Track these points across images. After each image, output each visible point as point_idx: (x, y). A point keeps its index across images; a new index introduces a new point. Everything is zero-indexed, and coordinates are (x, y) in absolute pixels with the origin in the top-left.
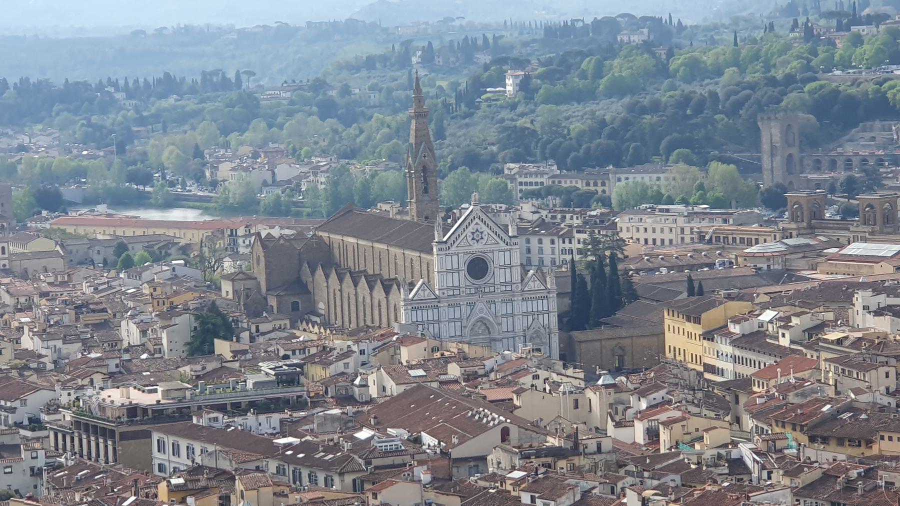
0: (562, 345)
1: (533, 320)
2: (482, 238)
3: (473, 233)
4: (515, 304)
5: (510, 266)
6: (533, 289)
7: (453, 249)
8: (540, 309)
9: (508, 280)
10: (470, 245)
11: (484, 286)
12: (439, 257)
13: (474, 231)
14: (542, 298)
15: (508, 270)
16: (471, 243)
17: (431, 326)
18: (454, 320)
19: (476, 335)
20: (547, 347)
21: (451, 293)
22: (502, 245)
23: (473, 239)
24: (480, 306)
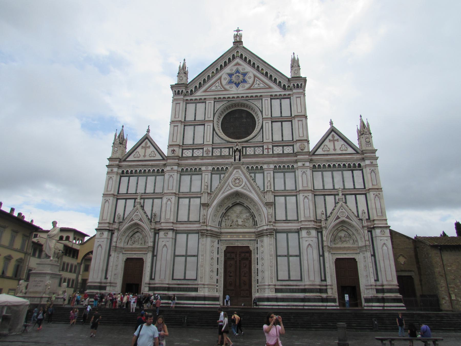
0: (402, 260)
1: (336, 203)
2: (244, 81)
3: (230, 75)
4: (299, 173)
6: (334, 152)
7: (199, 94)
8: (349, 185)
10: (226, 90)
12: (175, 102)
14: (352, 168)
15: (287, 125)
16: (227, 87)
17: (148, 203)
18: (190, 196)
20: (370, 259)
21: (188, 153)
22: (276, 89)
23: (230, 82)
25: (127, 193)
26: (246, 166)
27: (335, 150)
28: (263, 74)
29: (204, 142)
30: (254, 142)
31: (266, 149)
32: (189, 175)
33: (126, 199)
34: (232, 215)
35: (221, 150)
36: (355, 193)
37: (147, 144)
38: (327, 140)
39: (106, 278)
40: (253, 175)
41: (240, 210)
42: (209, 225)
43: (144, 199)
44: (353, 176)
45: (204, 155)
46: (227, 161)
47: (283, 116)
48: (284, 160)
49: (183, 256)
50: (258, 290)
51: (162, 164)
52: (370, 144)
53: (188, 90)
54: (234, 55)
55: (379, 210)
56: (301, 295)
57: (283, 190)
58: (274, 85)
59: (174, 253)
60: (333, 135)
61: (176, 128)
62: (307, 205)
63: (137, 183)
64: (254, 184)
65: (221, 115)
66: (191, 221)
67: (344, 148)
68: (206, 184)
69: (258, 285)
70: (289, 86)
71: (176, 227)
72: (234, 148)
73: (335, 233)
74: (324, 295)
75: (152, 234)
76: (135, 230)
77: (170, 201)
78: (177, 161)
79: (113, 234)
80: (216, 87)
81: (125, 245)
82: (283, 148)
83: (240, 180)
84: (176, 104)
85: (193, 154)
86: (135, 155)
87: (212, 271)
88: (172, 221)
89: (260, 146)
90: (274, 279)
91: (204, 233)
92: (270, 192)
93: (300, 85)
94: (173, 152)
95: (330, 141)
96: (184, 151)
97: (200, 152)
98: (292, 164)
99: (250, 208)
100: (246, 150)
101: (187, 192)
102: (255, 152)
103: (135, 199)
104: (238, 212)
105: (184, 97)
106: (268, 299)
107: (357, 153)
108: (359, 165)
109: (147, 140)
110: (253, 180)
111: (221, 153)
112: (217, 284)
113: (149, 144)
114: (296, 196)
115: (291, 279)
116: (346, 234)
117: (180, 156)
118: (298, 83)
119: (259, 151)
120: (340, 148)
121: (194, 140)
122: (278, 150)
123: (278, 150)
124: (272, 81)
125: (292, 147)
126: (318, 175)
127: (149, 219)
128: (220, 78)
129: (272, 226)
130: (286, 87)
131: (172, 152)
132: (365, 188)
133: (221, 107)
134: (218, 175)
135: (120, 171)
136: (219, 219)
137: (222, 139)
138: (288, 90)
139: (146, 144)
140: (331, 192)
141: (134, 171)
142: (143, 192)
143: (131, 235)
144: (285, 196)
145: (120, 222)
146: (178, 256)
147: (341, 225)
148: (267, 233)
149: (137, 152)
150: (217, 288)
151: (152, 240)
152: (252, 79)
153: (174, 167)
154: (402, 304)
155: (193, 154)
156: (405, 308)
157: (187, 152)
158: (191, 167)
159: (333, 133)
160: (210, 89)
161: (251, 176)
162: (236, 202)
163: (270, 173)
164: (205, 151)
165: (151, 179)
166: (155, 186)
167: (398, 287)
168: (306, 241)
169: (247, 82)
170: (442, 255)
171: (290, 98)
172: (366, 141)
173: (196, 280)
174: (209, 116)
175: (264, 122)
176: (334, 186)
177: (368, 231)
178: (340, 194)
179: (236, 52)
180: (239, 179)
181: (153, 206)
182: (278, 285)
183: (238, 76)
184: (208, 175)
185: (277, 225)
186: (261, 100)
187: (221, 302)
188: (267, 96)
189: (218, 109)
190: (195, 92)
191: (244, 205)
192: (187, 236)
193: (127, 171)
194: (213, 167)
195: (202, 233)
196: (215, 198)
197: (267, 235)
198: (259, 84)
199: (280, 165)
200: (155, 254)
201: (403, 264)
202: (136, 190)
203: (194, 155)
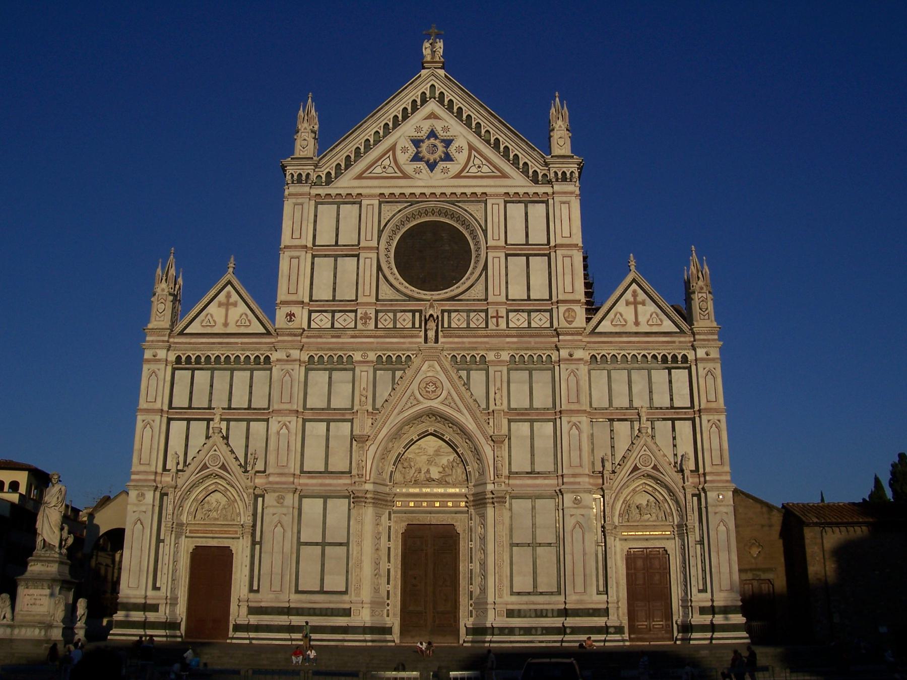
0: (755, 551)
2: (448, 158)
3: (417, 143)
4: (564, 371)
5: (547, 251)
7: (346, 183)
9: (539, 291)
10: (405, 176)
11: (448, 306)
13: (424, 134)
14: (670, 363)
15: (538, 264)
16: (409, 168)
17: (238, 430)
19: (416, 483)
22: (519, 183)
23: (416, 158)
24: (428, 370)
25: (190, 408)
26: (449, 354)
27: (637, 323)
28: (488, 142)
29: (357, 296)
30: (468, 300)
31: (492, 317)
32: (325, 369)
33: (189, 420)
34: (418, 459)
35: (395, 316)
36: (673, 415)
37: (230, 297)
38: (622, 301)
39: (155, 588)
40: (464, 374)
41: (435, 449)
42: (371, 481)
43: (228, 421)
44: (670, 382)
45: (360, 326)
46: (410, 343)
47: (530, 243)
48: (530, 343)
49: (317, 544)
50: (471, 611)
51: (266, 343)
52: (708, 313)
53: (320, 174)
54: (424, 93)
55: (716, 454)
56: (557, 622)
57: (526, 409)
58: (512, 171)
59: (299, 538)
60: (634, 292)
61: (294, 261)
62: (575, 443)
63: (212, 386)
64: (467, 395)
65: (395, 234)
66: (332, 473)
67: (655, 320)
68: (364, 393)
69: (471, 602)
70: (545, 175)
71: (300, 484)
72: (424, 313)
73: (628, 498)
74: (599, 621)
75: (249, 500)
76: (210, 488)
77: (287, 428)
78: (299, 338)
79: (163, 495)
80: (384, 168)
81: (190, 519)
82: (529, 316)
83: (438, 384)
84: (295, 204)
85: (333, 324)
86: (203, 320)
87: (377, 575)
88: (292, 471)
89: (481, 311)
90: (506, 590)
91: (362, 497)
92: (500, 413)
93: (568, 175)
94: (291, 318)
95: (628, 303)
96: (314, 315)
97: (349, 320)
98: (548, 353)
99: (456, 445)
100: (449, 317)
101: (323, 409)
102: (468, 324)
103: (209, 421)
104: (431, 451)
105: (311, 188)
106: (492, 630)
107: (682, 332)
108: (685, 357)
109: (229, 288)
110: (464, 385)
111: (395, 323)
112: (388, 601)
113: (235, 297)
114: (555, 421)
115: (540, 590)
116: (652, 499)
117: (306, 328)
118: (565, 170)
119: (478, 320)
120: (648, 322)
121: (334, 289)
122: (519, 320)
123: (518, 320)
124: (509, 161)
125: (547, 315)
126: (600, 377)
127: (240, 465)
128: (393, 148)
129: (503, 484)
130: (540, 178)
131: (288, 317)
132: (692, 406)
133: (394, 215)
134: (390, 372)
135: (172, 357)
136: (391, 468)
137: (398, 290)
138: (542, 184)
139: (228, 296)
140: (624, 415)
141: (203, 359)
142: (227, 406)
143: (201, 497)
144: (532, 422)
145: (178, 471)
146: (306, 544)
147: (644, 481)
148: (493, 498)
149: (207, 315)
150: (388, 608)
151: (251, 509)
152: (465, 153)
153: (292, 352)
154: (745, 634)
155: (333, 324)
156: (748, 641)
157: (320, 318)
158: (331, 353)
159: (634, 286)
160: (370, 173)
161: (460, 377)
162: (427, 431)
163: (501, 371)
164: (361, 318)
165: (242, 377)
166: (251, 393)
167: (740, 604)
168: (571, 515)
169: (453, 161)
170: (825, 541)
171: (546, 202)
172: (700, 309)
173: (345, 592)
174: (369, 238)
175: (490, 255)
176: (631, 401)
177: (693, 495)
178: (644, 419)
179: (429, 85)
180: (435, 384)
181: (247, 438)
182: (512, 604)
183: (435, 146)
184: (367, 371)
185: (511, 482)
186: (483, 204)
187: (395, 637)
188: (497, 195)
189: (389, 221)
190: (336, 178)
191: (445, 438)
192: (325, 503)
193: (189, 357)
194: (379, 353)
195: (358, 497)
196: (384, 423)
197: (493, 503)
198: (479, 167)
199: (522, 353)
200: (258, 539)
201: (755, 558)
202: (210, 401)
203: (336, 325)
